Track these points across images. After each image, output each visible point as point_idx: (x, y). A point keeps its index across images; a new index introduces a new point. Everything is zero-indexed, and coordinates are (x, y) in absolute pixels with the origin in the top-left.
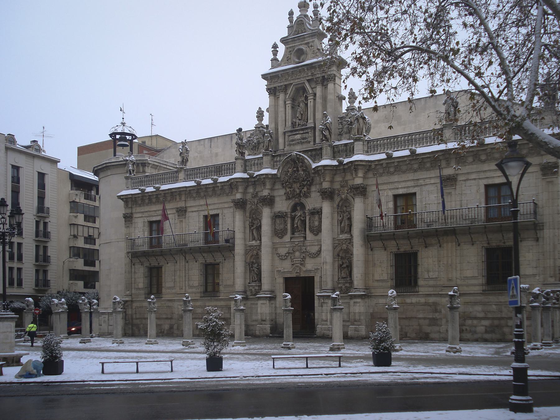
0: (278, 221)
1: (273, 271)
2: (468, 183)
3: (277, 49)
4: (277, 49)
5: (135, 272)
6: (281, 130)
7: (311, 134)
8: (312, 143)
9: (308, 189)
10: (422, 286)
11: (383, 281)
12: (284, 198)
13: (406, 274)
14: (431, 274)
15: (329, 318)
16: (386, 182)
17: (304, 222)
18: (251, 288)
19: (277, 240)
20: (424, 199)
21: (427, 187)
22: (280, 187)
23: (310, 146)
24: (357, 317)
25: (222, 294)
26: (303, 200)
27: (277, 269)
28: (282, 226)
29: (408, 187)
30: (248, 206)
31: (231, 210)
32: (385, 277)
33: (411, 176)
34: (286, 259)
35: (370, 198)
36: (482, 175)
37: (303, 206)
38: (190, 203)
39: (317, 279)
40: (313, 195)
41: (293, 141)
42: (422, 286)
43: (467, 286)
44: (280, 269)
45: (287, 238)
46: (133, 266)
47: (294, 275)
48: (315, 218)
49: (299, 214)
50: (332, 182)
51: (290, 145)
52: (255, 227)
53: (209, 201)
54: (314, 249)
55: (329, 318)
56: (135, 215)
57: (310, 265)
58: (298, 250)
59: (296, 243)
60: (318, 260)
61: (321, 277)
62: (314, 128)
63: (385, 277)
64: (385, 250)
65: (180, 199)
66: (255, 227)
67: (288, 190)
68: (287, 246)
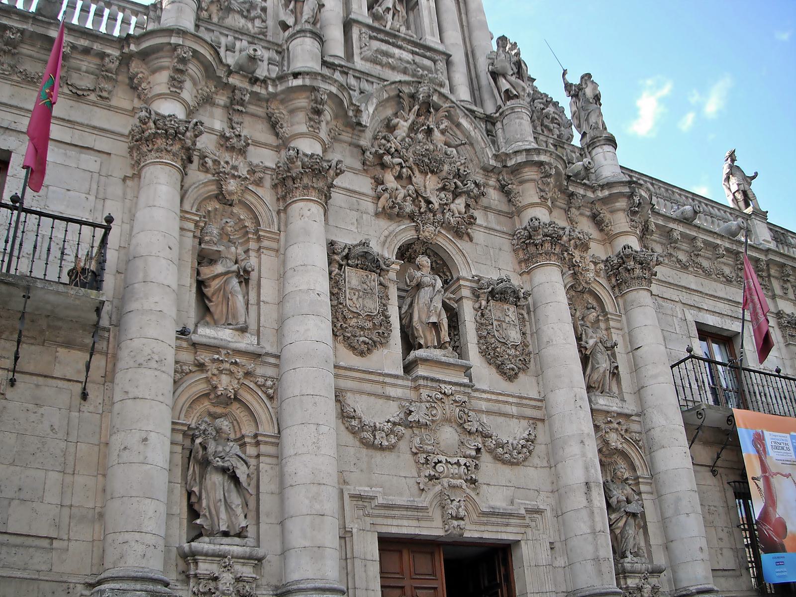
0: (353, 277)
18: (205, 567)
26: (445, 241)
28: (372, 305)
31: (90, 162)
34: (392, 448)
40: (479, 235)
41: (386, 54)
44: (364, 490)
47: (433, 529)
51: (374, 61)
57: (498, 487)
58: (448, 420)
59: (448, 389)
60: (532, 475)
68: (392, 392)
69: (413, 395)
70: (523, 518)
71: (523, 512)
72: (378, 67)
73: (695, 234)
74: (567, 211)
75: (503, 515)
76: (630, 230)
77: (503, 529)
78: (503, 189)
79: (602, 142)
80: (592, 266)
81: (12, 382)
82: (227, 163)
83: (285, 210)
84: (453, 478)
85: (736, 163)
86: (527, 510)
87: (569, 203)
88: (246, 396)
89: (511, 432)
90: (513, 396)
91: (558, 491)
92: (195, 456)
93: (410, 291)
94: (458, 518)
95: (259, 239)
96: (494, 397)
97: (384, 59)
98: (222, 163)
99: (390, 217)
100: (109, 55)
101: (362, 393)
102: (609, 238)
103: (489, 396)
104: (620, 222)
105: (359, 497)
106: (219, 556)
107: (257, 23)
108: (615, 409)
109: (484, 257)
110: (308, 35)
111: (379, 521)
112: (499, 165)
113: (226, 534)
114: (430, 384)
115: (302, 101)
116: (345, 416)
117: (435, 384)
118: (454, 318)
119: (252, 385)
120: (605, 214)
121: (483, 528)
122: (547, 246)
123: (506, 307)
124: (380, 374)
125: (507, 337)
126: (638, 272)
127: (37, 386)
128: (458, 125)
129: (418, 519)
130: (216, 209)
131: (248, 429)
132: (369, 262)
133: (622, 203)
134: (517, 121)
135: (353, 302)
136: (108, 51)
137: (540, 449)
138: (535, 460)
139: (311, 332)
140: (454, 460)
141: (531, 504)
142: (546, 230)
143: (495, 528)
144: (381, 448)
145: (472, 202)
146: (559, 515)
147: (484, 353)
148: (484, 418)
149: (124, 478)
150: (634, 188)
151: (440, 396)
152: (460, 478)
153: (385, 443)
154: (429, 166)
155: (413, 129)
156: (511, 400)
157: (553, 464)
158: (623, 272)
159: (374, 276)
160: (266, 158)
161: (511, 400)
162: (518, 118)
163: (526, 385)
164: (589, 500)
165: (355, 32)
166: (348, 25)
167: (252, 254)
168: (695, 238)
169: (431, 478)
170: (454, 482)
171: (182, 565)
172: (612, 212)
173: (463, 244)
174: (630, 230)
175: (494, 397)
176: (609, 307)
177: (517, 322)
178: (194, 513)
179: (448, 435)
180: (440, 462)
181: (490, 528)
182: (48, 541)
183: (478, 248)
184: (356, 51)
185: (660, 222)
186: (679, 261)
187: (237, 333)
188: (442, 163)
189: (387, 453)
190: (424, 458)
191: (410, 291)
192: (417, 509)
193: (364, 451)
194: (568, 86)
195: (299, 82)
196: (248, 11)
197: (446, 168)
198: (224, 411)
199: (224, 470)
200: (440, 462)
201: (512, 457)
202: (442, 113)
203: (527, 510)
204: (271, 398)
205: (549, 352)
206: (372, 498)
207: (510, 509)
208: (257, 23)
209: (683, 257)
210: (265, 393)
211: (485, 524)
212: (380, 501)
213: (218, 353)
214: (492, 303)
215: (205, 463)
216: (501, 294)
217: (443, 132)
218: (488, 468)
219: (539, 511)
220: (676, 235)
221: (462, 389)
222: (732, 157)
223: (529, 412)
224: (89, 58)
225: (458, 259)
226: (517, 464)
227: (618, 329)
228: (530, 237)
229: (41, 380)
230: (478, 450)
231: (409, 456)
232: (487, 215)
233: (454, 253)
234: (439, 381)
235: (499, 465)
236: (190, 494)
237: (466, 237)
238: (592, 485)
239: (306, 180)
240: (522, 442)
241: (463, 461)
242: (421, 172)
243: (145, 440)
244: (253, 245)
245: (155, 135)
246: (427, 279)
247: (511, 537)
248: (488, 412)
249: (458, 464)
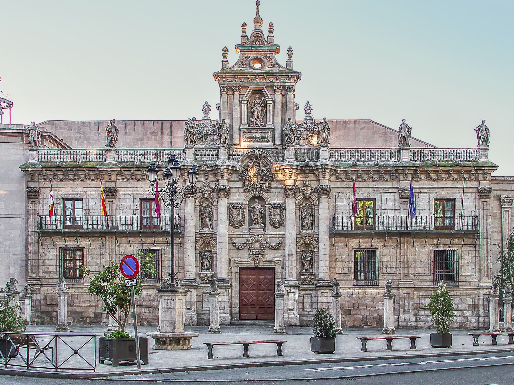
0: (235, 212)
1: (229, 260)
2: (421, 195)
3: (292, 52)
4: (292, 52)
5: (43, 253)
6: (236, 126)
7: (270, 135)
8: (271, 143)
9: (269, 184)
10: (381, 280)
11: (344, 275)
12: (242, 190)
13: (366, 268)
14: (389, 269)
15: (296, 307)
17: (263, 217)
19: (233, 230)
20: (383, 205)
21: (386, 194)
22: (237, 179)
23: (270, 145)
26: (263, 194)
27: (233, 259)
29: (368, 193)
30: (199, 194)
32: (346, 271)
33: (371, 184)
34: (243, 249)
35: (332, 200)
36: (432, 190)
38: (123, 184)
39: (278, 270)
40: (273, 190)
42: (381, 280)
43: (420, 281)
45: (244, 229)
46: (41, 247)
47: (252, 265)
49: (259, 207)
50: (295, 180)
52: (206, 216)
53: (55, 185)
54: (275, 242)
55: (296, 307)
56: (42, 191)
57: (269, 256)
60: (280, 252)
61: (283, 268)
62: (274, 130)
63: (346, 271)
65: (110, 179)
66: (206, 216)
68: (244, 236)
69: (249, 236)
92: (200, 255)
109: (273, 197)
133: (320, 170)
135: (234, 217)
141: (277, 259)
149: (186, 263)
163: (281, 230)
173: (269, 194)
179: (257, 245)
197: (262, 174)
216: (275, 207)
218: (267, 251)
220: (349, 172)
223: (281, 236)
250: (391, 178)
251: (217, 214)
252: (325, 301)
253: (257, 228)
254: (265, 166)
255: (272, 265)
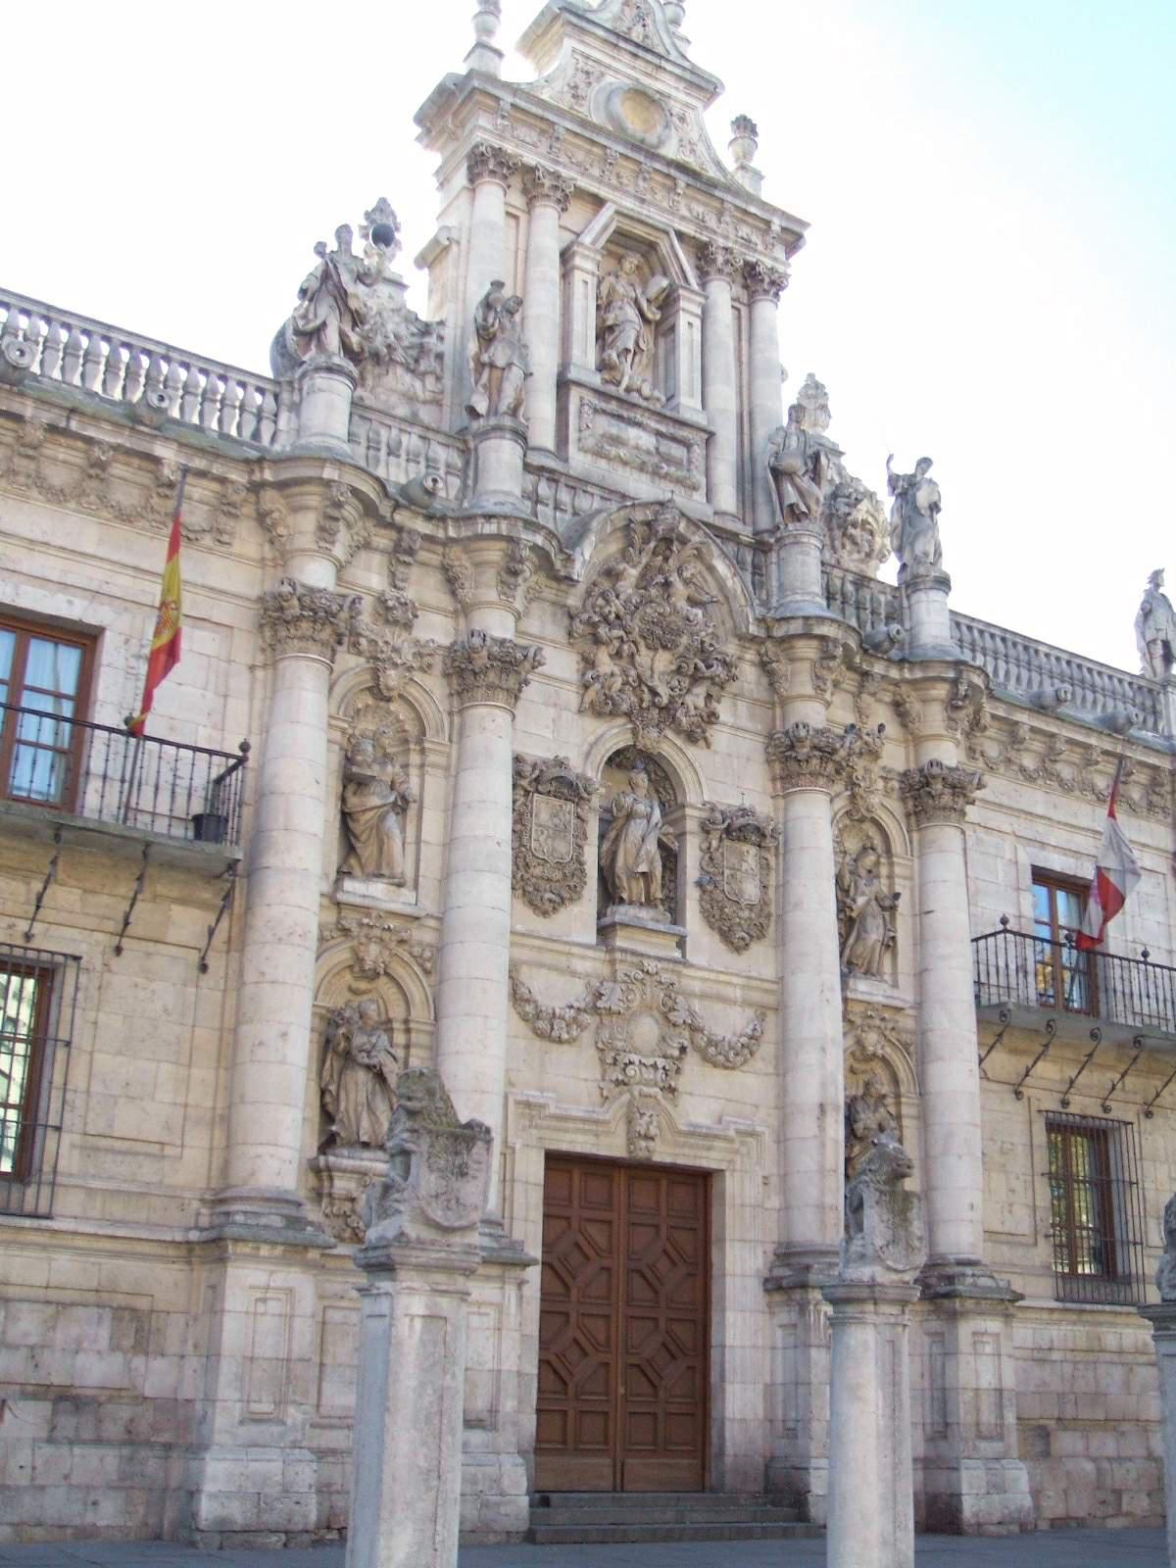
0: (543, 808)
9: (709, 697)
12: (571, 697)
16: (1005, 801)
24: (988, 1416)
25: (69, 1203)
26: (670, 747)
28: (564, 848)
34: (572, 1041)
37: (664, 781)
40: (719, 736)
41: (616, 441)
44: (534, 1095)
47: (613, 1145)
48: (742, 859)
51: (599, 453)
60: (751, 1084)
64: (1018, 1094)
67: (606, 664)
68: (580, 966)
70: (730, 1140)
71: (732, 1133)
72: (603, 463)
73: (1054, 730)
74: (857, 696)
75: (706, 1136)
76: (944, 732)
77: (704, 1153)
78: (764, 665)
79: (929, 585)
80: (880, 784)
81: (118, 950)
82: (387, 643)
83: (461, 712)
84: (646, 1085)
85: (1161, 590)
86: (738, 1132)
87: (861, 686)
88: (398, 970)
89: (728, 1022)
90: (737, 975)
91: (784, 1108)
93: (613, 823)
94: (648, 1138)
95: (423, 751)
96: (712, 976)
97: (613, 451)
98: (381, 644)
99: (598, 714)
100: (232, 482)
101: (541, 965)
102: (915, 739)
103: (706, 974)
104: (934, 717)
105: (528, 1105)
106: (359, 1173)
107: (430, 381)
108: (881, 999)
109: (725, 771)
110: (508, 435)
111: (548, 1134)
112: (762, 634)
113: (366, 1145)
114: (629, 958)
115: (494, 553)
116: (518, 996)
117: (635, 959)
118: (671, 858)
119: (407, 957)
120: (914, 706)
121: (677, 1151)
122: (815, 762)
123: (745, 847)
124: (566, 943)
125: (740, 893)
126: (947, 799)
127: (148, 954)
128: (711, 569)
129: (597, 1136)
130: (367, 706)
131: (397, 1012)
132: (569, 789)
134: (800, 557)
135: (540, 843)
136: (233, 476)
137: (766, 1049)
138: (757, 1064)
139: (487, 895)
140: (651, 1061)
142: (816, 741)
143: (692, 1153)
144: (560, 1041)
145: (715, 691)
146: (782, 1140)
147: (703, 911)
148: (697, 1005)
150: (961, 672)
151: (641, 975)
152: (656, 1085)
153: (565, 1036)
154: (661, 637)
155: (644, 581)
156: (735, 980)
157: (782, 1069)
158: (928, 795)
159: (570, 806)
160: (436, 630)
161: (735, 980)
162: (802, 553)
163: (759, 960)
164: (822, 1128)
165: (575, 395)
166: (563, 385)
167: (414, 772)
168: (1053, 736)
169: (618, 1083)
170: (646, 1090)
171: (312, 1181)
172: (924, 701)
174: (944, 732)
175: (712, 976)
176: (897, 847)
177: (757, 870)
178: (327, 1116)
179: (647, 1030)
180: (631, 1063)
181: (687, 1151)
182: (158, 1146)
183: (718, 758)
184: (573, 435)
185: (1001, 713)
186: (1023, 770)
187: (393, 888)
188: (679, 633)
189: (565, 1047)
190: (612, 1058)
191: (613, 823)
192: (596, 1122)
193: (538, 1043)
194: (893, 481)
195: (490, 528)
196: (417, 361)
197: (684, 640)
198: (369, 986)
199: (368, 1068)
200: (631, 1063)
201: (724, 1056)
202: (689, 551)
203: (738, 1132)
204: (427, 972)
205: (798, 918)
206: (543, 1106)
207: (717, 1130)
208: (430, 381)
209: (1029, 762)
210: (421, 966)
211: (684, 1145)
212: (552, 1110)
213: (368, 915)
214: (727, 842)
215: (348, 1057)
216: (739, 829)
217: (687, 582)
219: (752, 1134)
220: (1024, 732)
221: (671, 966)
222: (1156, 578)
224: (204, 483)
225: (687, 776)
226: (733, 1068)
227: (905, 878)
228: (792, 747)
229: (151, 947)
230: (683, 1049)
231: (593, 1053)
232: (735, 705)
233: (683, 765)
234: (642, 955)
235: (708, 1069)
236: (323, 1092)
237: (702, 743)
238: (829, 1109)
239: (492, 677)
240: (744, 1040)
241: (661, 1062)
242: (648, 647)
243: (284, 1035)
244: (415, 758)
245: (299, 618)
246: (641, 808)
247: (713, 1165)
248: (704, 996)
249: (655, 1066)
250: (1151, 806)
251: (452, 809)
252: (987, 1380)
253: (644, 938)
254: (693, 602)
255: (707, 1160)
